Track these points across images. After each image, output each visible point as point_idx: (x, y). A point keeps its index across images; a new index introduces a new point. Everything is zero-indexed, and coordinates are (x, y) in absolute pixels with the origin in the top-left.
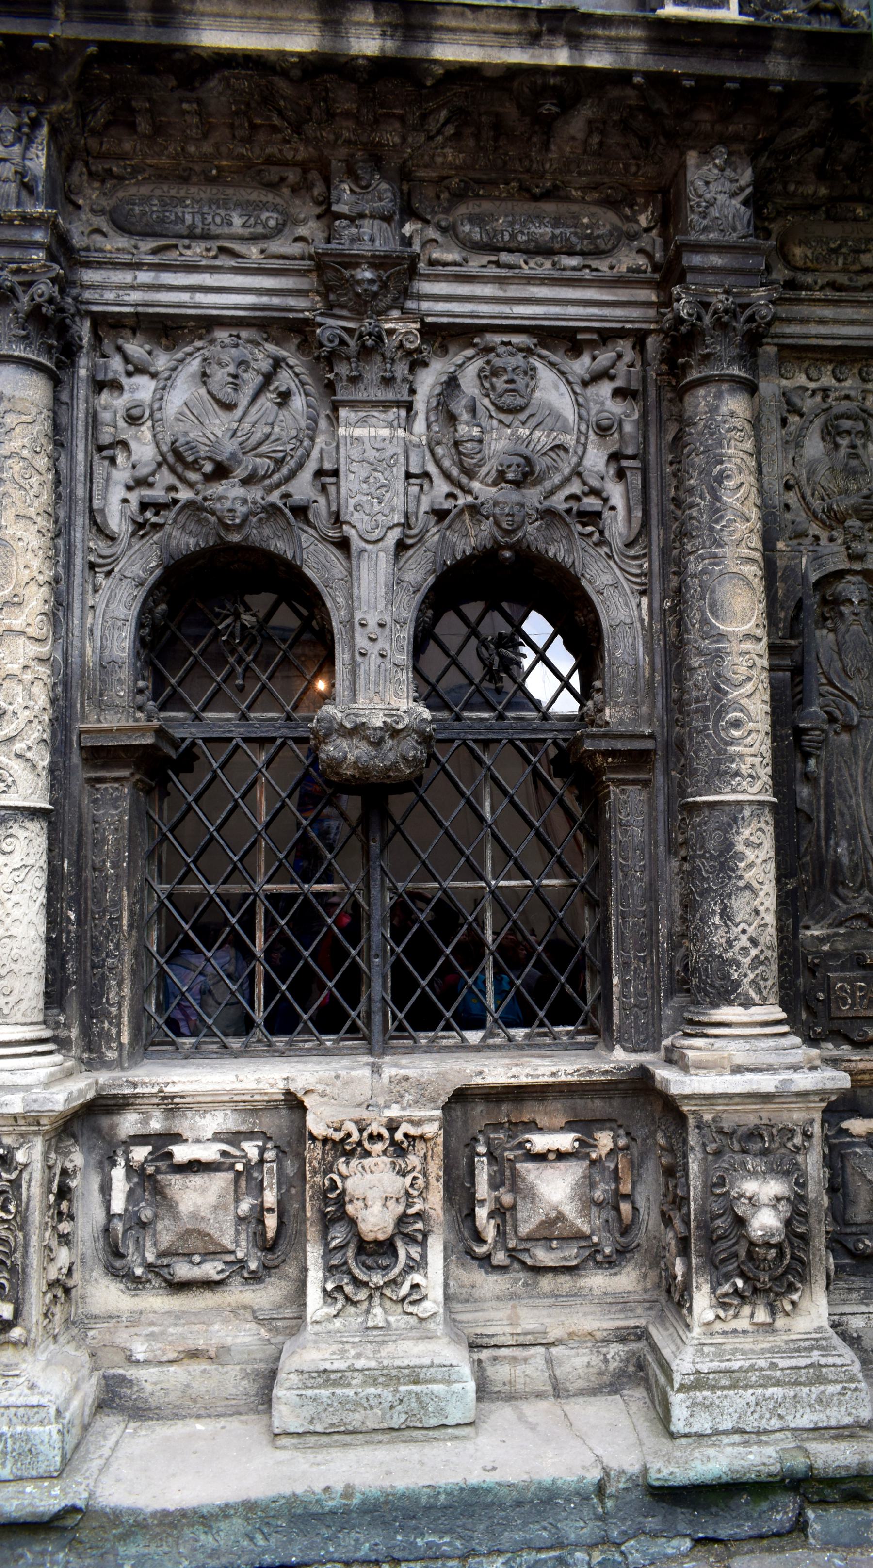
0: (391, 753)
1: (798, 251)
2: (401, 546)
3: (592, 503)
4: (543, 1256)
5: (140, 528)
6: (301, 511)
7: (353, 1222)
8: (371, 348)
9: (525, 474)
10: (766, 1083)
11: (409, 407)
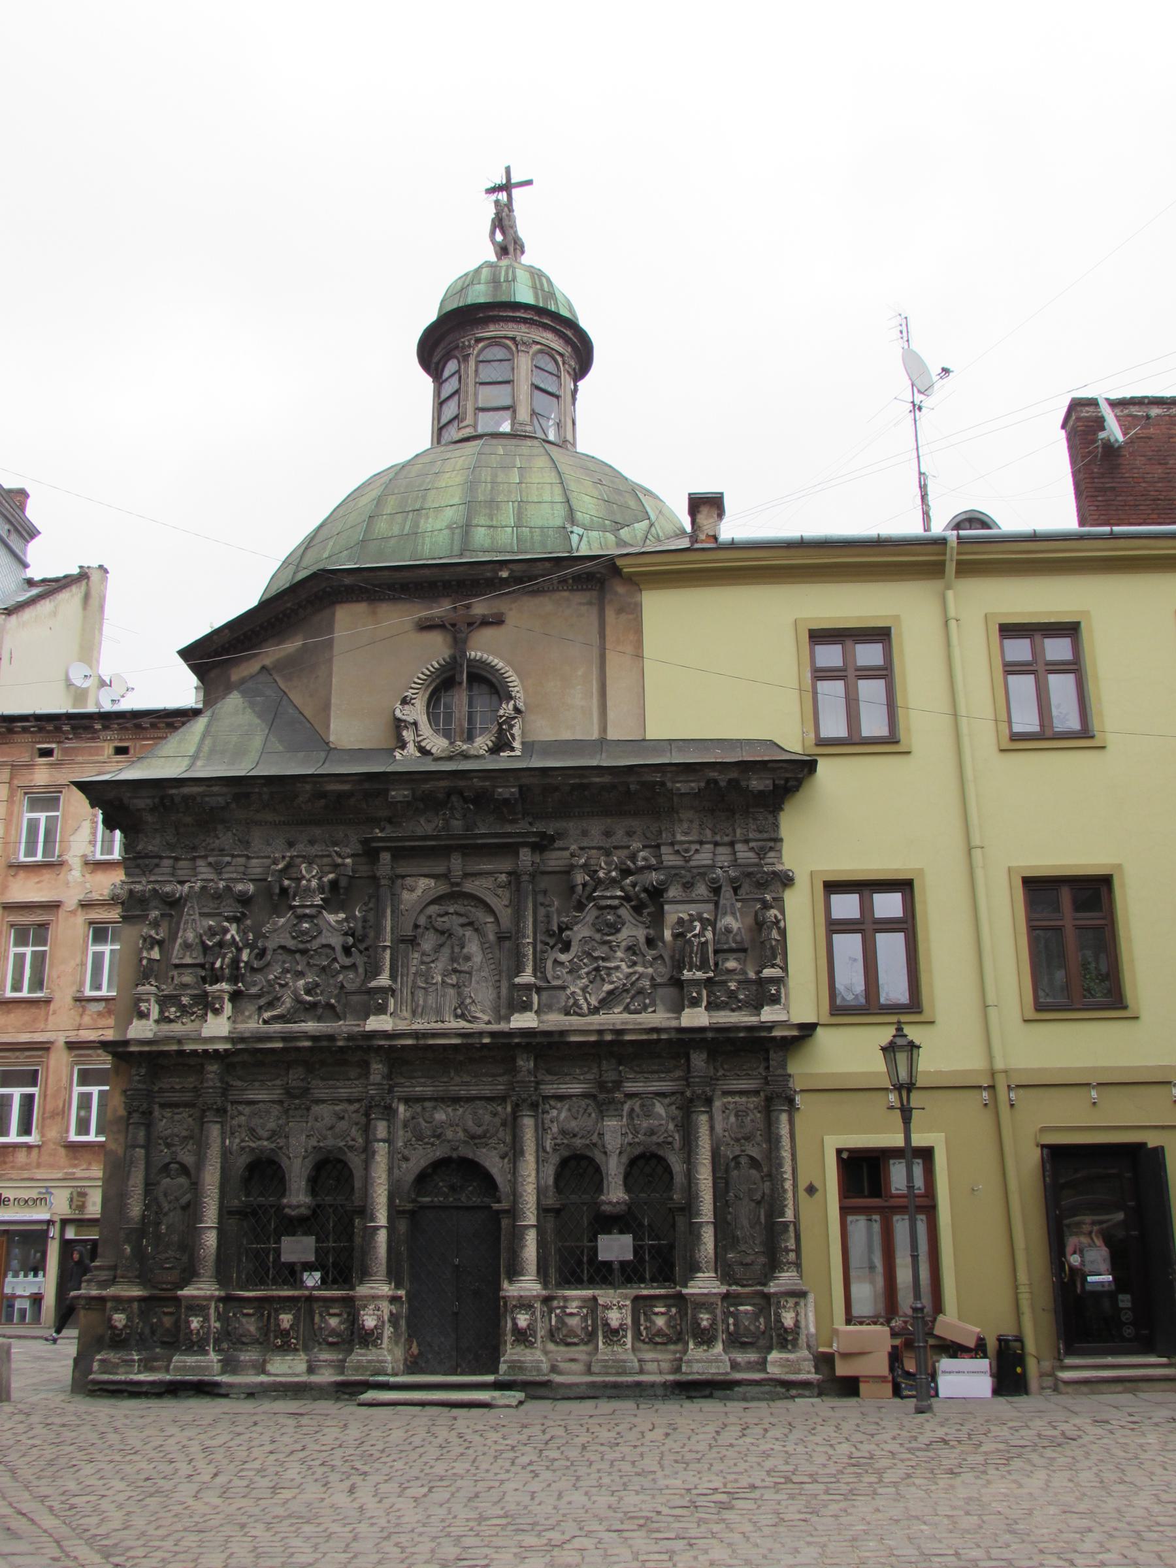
0: (618, 1209)
1: (726, 1067)
2: (620, 1153)
3: (670, 1139)
4: (658, 1340)
5: (555, 1150)
6: (595, 1145)
7: (608, 1325)
8: (612, 1101)
9: (651, 1132)
10: (705, 1291)
11: (622, 1116)
